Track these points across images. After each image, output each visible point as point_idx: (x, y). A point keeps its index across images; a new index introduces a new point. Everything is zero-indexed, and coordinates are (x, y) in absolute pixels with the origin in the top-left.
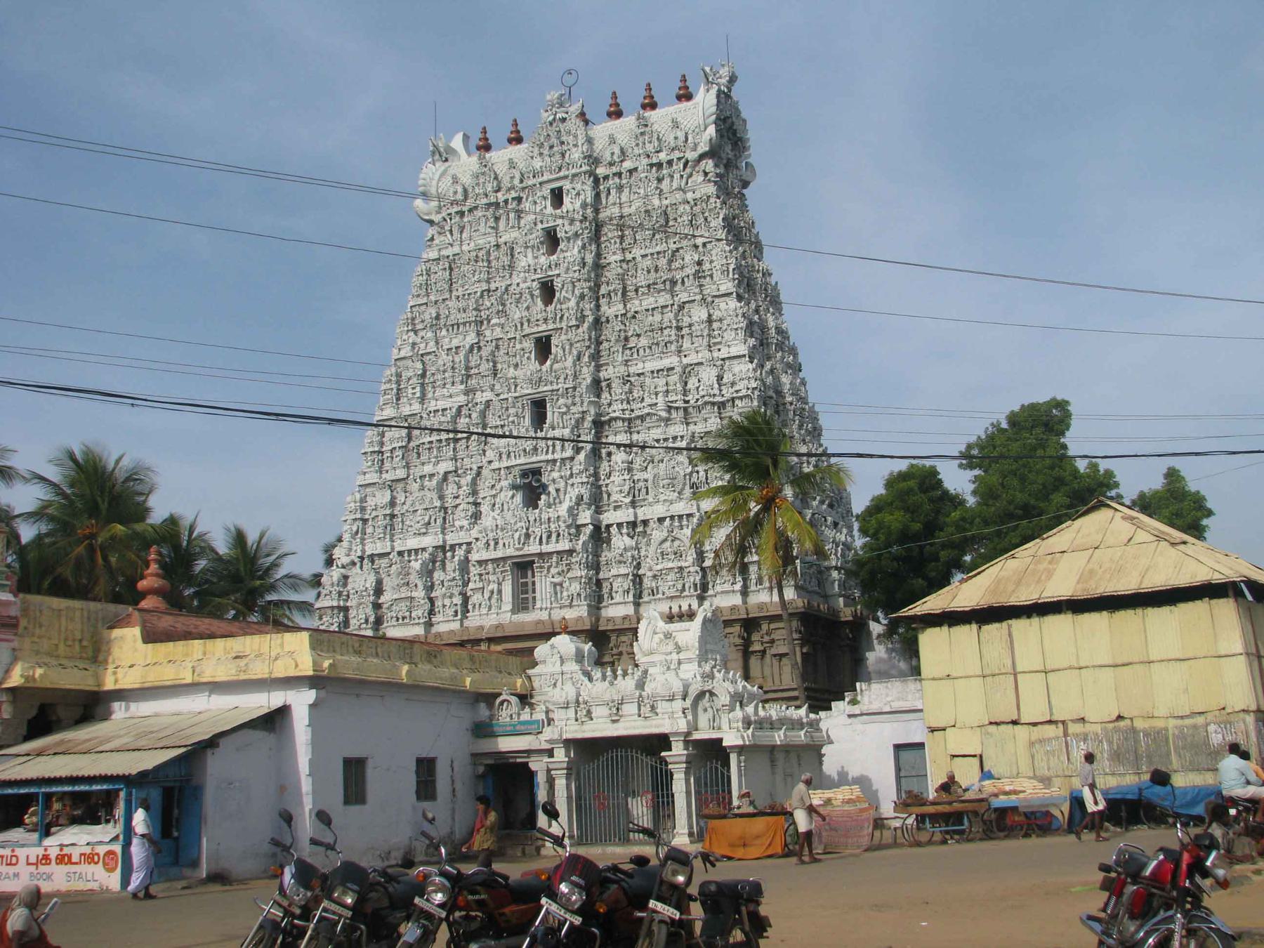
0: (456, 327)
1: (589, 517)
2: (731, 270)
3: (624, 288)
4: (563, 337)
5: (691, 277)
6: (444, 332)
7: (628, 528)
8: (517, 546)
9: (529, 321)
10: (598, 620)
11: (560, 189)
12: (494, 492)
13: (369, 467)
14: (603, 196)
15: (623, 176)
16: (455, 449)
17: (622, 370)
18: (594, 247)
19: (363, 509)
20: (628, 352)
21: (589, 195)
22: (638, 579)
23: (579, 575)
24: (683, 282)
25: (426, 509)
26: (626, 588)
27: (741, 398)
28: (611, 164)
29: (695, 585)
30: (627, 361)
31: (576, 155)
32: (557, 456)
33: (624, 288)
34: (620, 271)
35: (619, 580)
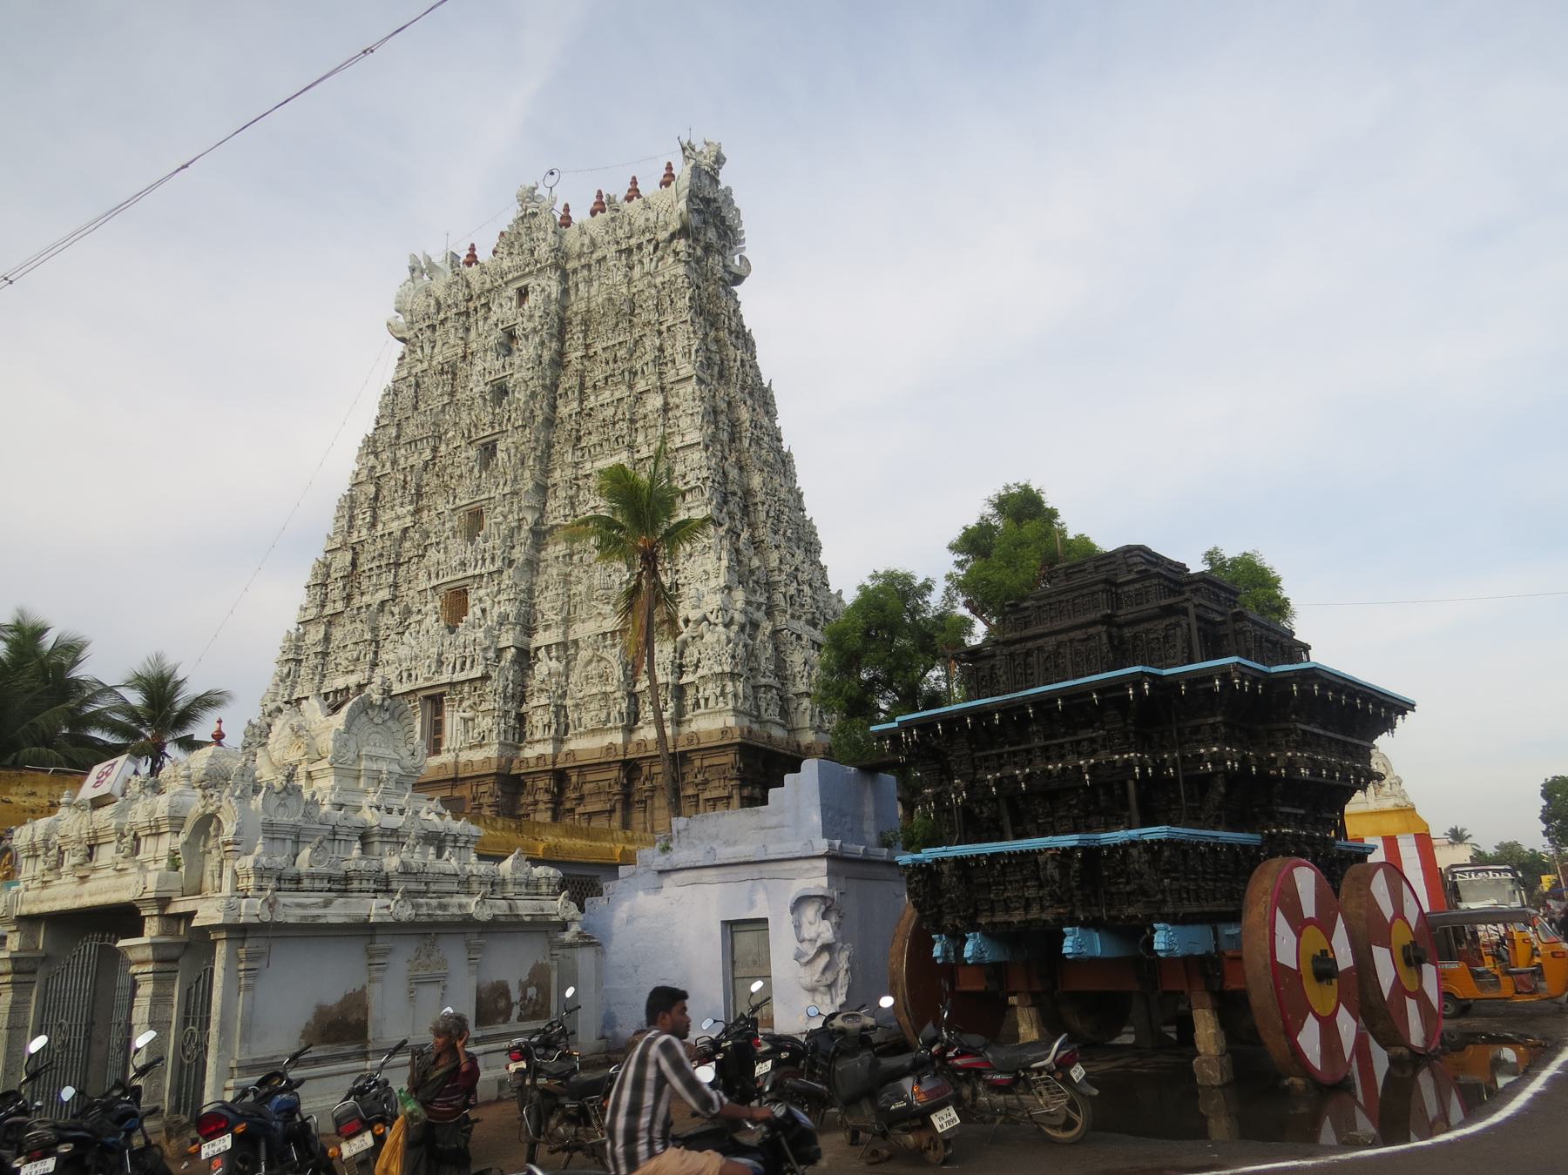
0: (413, 445)
1: (511, 639)
2: (693, 352)
3: (582, 385)
4: (509, 440)
5: (650, 364)
6: (403, 451)
7: (557, 650)
8: (427, 675)
9: (475, 426)
10: (511, 761)
11: (526, 287)
12: (420, 617)
13: (311, 602)
14: (572, 292)
15: (593, 268)
16: (395, 576)
17: (569, 472)
18: (554, 345)
19: (298, 648)
20: (579, 453)
21: (554, 289)
22: (560, 709)
23: (491, 707)
24: (643, 372)
25: (356, 643)
26: (546, 721)
27: (691, 490)
28: (580, 256)
29: (620, 713)
30: (577, 463)
31: (543, 251)
32: (483, 571)
33: (582, 385)
34: (580, 367)
35: (540, 711)
